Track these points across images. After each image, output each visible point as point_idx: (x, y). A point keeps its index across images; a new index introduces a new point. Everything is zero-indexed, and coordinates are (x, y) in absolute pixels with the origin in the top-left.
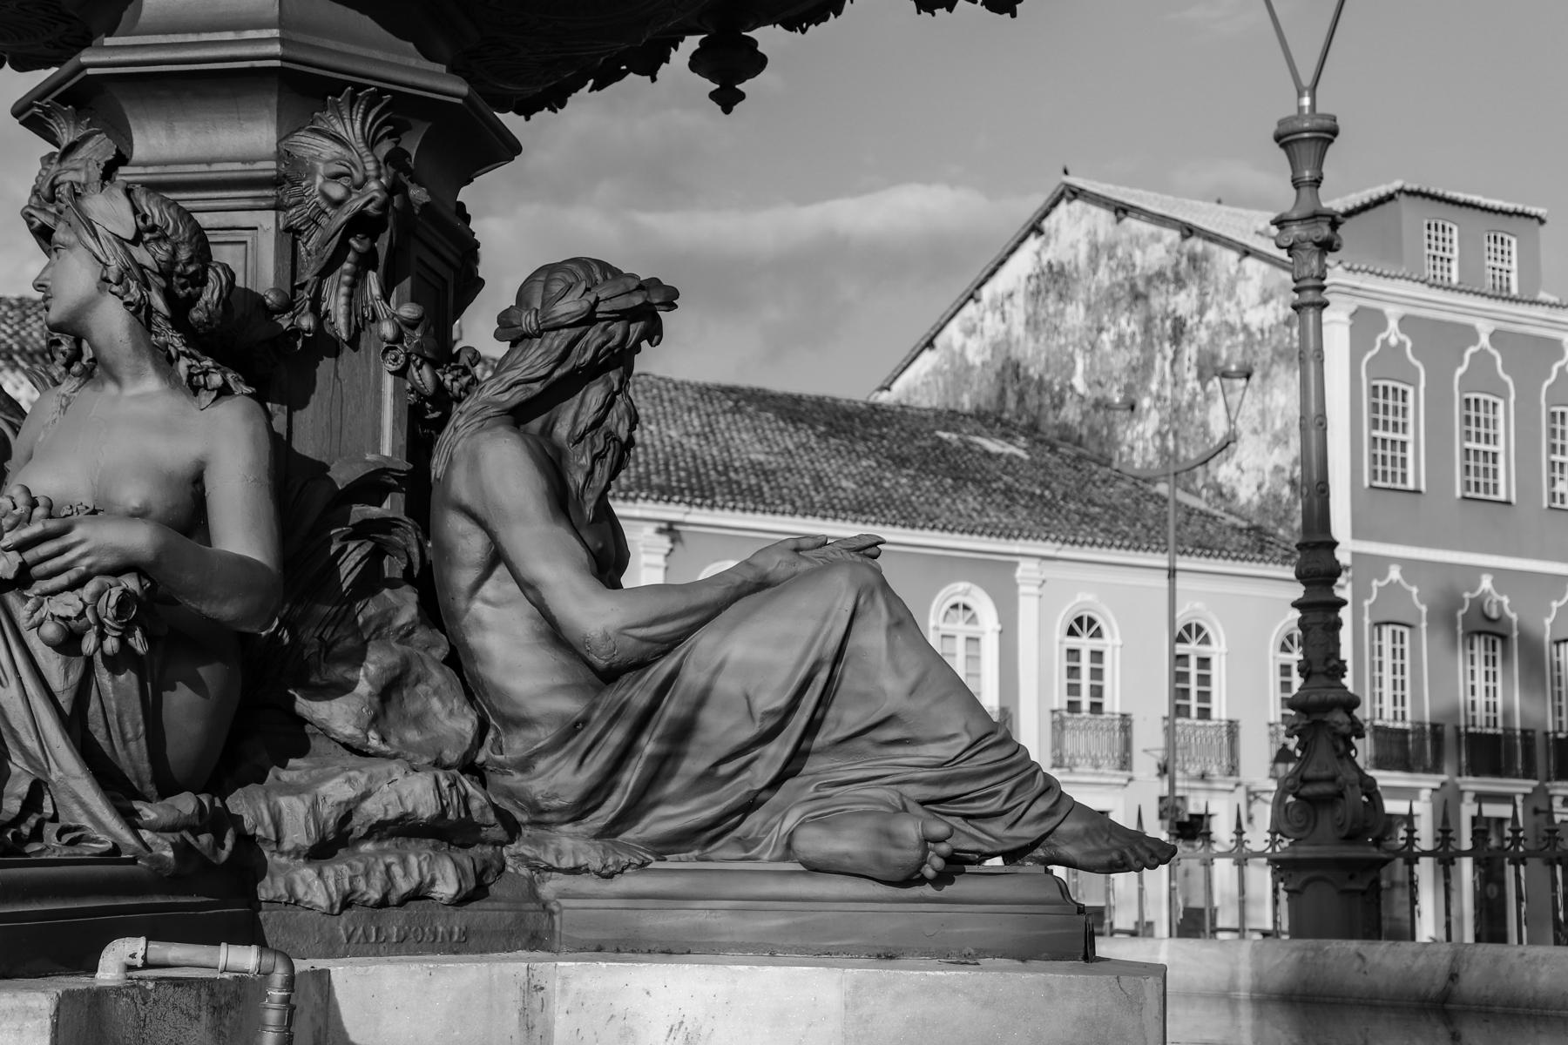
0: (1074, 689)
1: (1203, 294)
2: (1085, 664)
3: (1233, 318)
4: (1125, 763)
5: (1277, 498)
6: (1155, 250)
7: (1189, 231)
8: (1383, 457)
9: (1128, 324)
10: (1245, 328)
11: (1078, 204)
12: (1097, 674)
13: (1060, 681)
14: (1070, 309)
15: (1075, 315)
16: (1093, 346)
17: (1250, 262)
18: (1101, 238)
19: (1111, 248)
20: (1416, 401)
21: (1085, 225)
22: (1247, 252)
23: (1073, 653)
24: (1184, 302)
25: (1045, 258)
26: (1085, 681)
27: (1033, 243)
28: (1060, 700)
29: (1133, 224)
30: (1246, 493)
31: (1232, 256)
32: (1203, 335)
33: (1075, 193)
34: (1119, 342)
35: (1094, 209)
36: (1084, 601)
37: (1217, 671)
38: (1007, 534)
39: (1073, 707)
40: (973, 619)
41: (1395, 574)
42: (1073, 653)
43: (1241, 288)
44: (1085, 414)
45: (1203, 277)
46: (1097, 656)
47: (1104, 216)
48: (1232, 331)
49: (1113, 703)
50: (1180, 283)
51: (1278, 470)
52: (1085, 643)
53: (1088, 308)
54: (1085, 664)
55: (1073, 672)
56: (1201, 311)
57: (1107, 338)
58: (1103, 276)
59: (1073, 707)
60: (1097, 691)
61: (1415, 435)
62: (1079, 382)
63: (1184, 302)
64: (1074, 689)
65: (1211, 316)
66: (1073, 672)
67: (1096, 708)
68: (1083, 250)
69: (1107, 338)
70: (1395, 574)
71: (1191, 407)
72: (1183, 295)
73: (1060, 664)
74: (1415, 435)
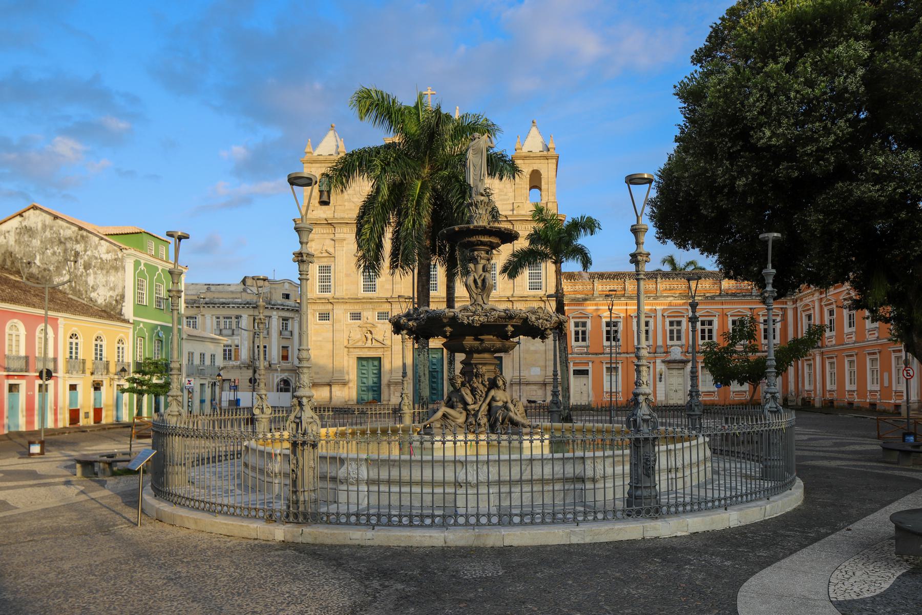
0: (71, 353)
1: (86, 247)
2: (74, 346)
3: (97, 255)
4: (84, 372)
5: (111, 304)
6: (71, 231)
7: (81, 228)
8: (139, 296)
9: (59, 250)
10: (101, 258)
11: (38, 212)
12: (77, 349)
13: (68, 350)
14: (34, 241)
15: (36, 243)
16: (43, 253)
17: (103, 242)
18: (47, 223)
19: (51, 228)
20: (146, 283)
21: (40, 218)
22: (102, 239)
23: (71, 343)
24: (79, 248)
25: (24, 224)
26: (74, 351)
27: (19, 219)
28: (68, 356)
29: (59, 222)
30: (100, 301)
31: (97, 239)
32: (86, 258)
33: (35, 208)
34: (54, 253)
35: (44, 214)
36: (74, 330)
37: (104, 348)
38: (58, 311)
39: (71, 357)
40: (18, 330)
41: (141, 325)
42: (71, 343)
43: (99, 248)
44: (40, 272)
45: (86, 242)
46: (77, 344)
47: (48, 219)
48: (96, 258)
49: (80, 356)
50: (77, 242)
51: (111, 297)
52: (74, 341)
53: (41, 242)
54: (74, 346)
55: (71, 348)
56: (86, 251)
57: (49, 252)
58: (48, 234)
59: (71, 357)
60: (77, 353)
61: (146, 292)
62: (37, 262)
63: (79, 248)
64: (71, 353)
65: (89, 253)
66: (71, 348)
67: (76, 358)
68: (40, 226)
69: (49, 252)
70: (141, 325)
71: (81, 276)
72: (78, 246)
73: (68, 346)
74: (146, 292)
